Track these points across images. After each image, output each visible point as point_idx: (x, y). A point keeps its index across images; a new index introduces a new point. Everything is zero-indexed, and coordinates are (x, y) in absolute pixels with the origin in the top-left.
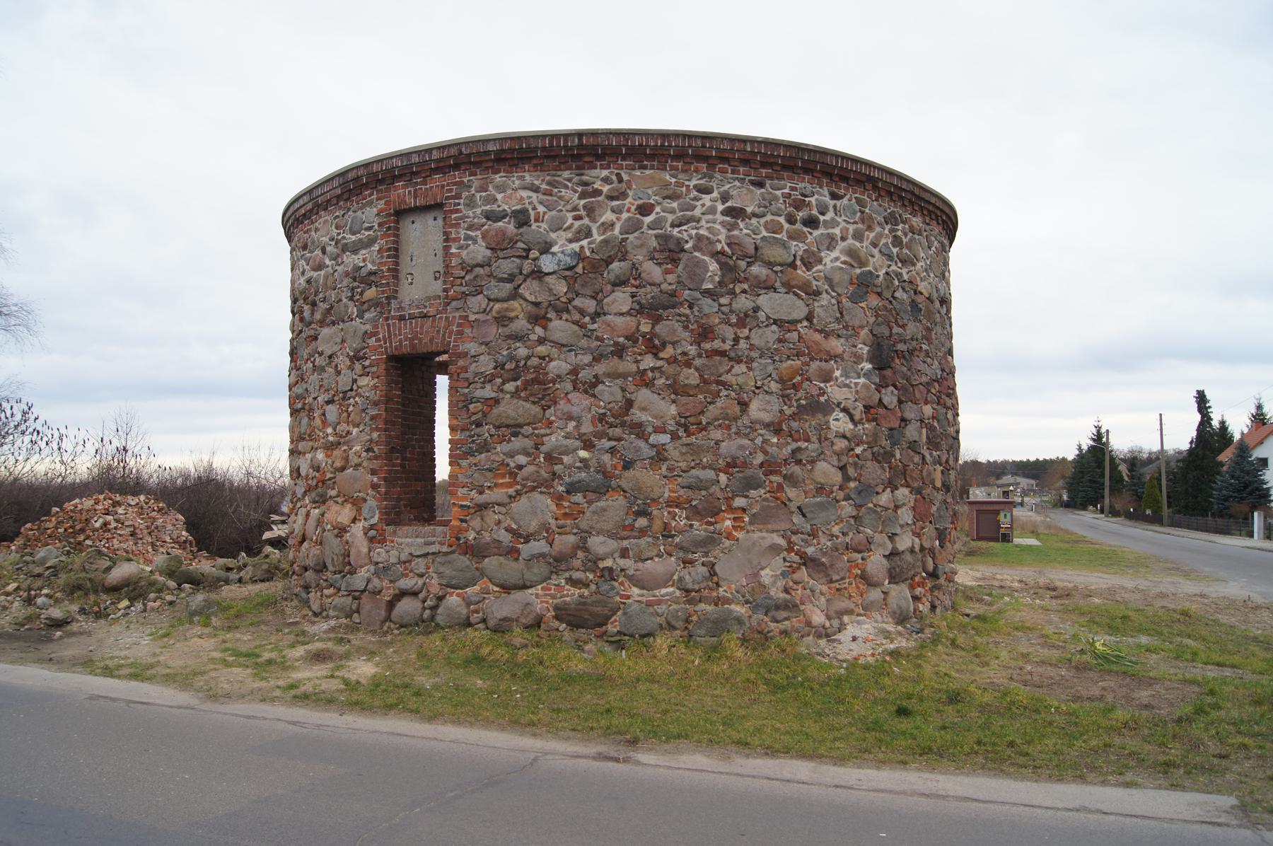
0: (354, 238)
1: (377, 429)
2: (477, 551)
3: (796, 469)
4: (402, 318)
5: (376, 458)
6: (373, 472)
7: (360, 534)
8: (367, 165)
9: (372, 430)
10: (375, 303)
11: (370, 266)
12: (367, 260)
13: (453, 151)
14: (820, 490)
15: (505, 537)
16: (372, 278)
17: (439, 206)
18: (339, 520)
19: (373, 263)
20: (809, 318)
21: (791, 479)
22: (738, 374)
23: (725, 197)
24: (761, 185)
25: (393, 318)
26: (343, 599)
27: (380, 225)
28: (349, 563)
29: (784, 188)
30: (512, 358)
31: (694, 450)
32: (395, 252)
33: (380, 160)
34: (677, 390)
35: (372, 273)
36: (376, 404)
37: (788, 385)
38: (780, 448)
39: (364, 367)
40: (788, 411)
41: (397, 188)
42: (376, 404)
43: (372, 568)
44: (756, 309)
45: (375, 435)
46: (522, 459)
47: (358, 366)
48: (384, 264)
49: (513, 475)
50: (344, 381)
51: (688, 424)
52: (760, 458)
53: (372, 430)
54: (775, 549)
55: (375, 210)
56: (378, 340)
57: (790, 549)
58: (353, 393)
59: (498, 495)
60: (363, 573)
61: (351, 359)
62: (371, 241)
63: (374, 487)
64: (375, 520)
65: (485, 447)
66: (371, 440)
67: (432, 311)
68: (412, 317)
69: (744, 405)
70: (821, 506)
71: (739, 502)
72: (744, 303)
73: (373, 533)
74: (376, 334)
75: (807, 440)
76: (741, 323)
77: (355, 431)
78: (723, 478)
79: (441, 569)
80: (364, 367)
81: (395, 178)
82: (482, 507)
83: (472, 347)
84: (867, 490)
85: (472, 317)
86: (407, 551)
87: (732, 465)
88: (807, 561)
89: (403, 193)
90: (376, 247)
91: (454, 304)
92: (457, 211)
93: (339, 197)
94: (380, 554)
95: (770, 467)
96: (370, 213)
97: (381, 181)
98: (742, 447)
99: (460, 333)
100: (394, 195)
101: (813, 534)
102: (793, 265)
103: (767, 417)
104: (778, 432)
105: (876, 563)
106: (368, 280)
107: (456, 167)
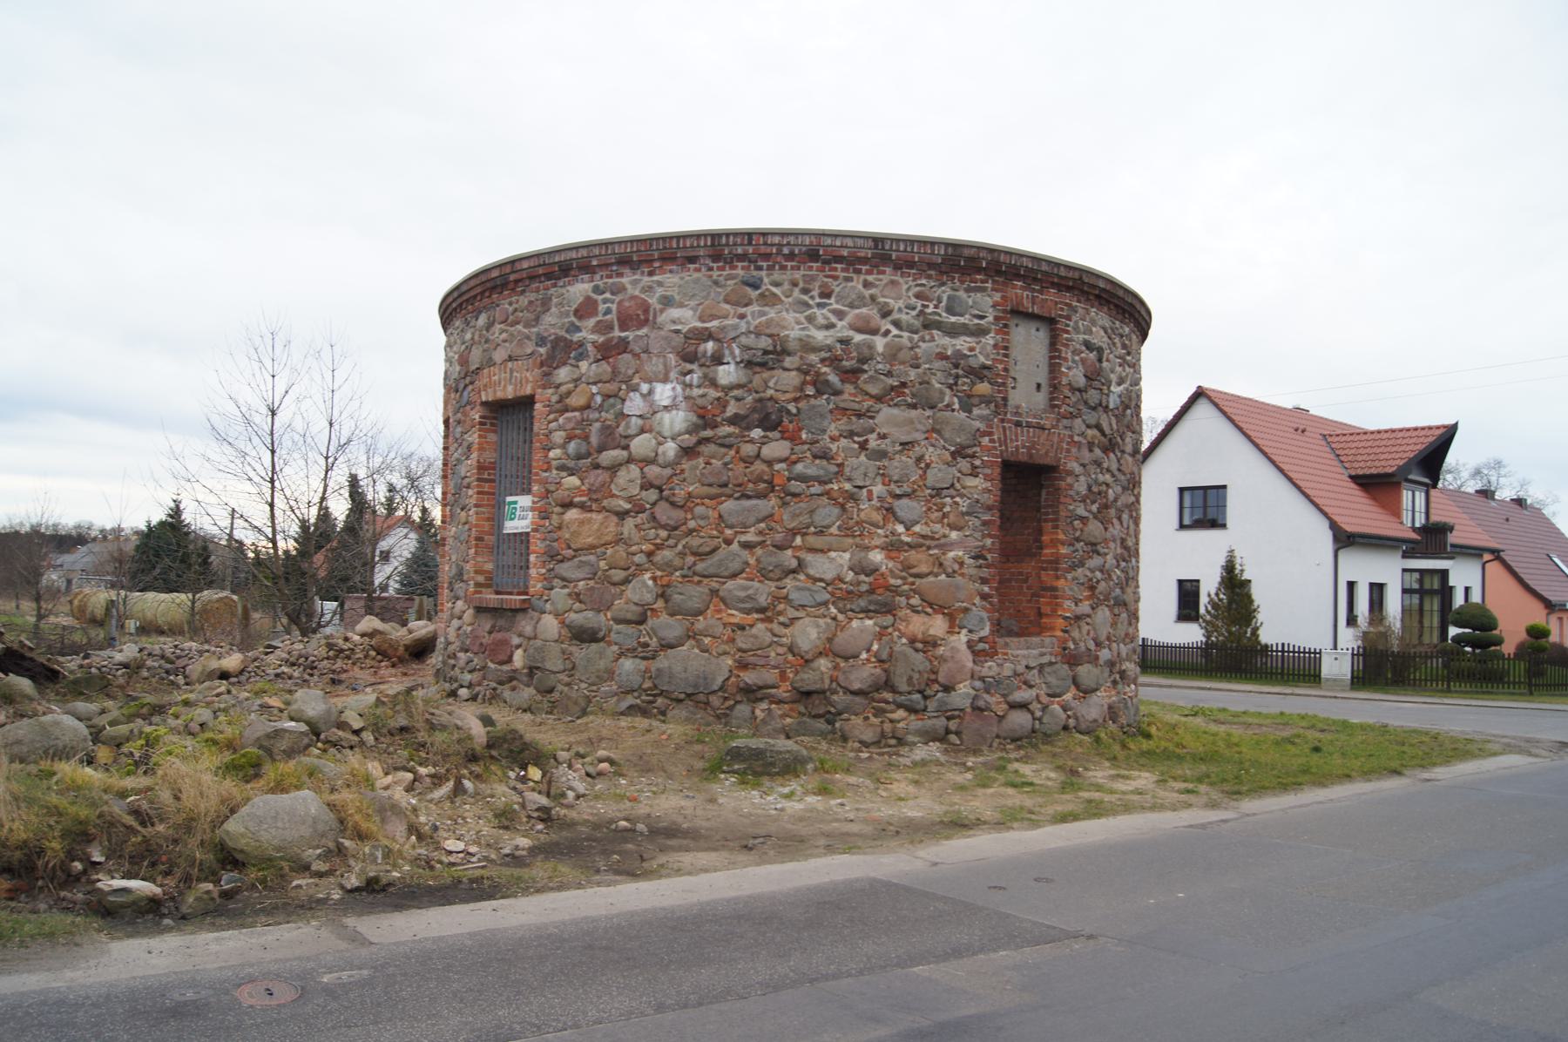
0: (953, 319)
1: (990, 536)
2: (1073, 660)
4: (1018, 424)
5: (988, 566)
6: (984, 581)
7: (964, 647)
8: (992, 250)
9: (984, 536)
10: (986, 400)
11: (982, 359)
12: (981, 351)
13: (1076, 275)
15: (1092, 645)
16: (986, 372)
17: (1050, 322)
18: (932, 632)
19: (987, 356)
25: (1009, 421)
26: (934, 721)
27: (997, 318)
28: (936, 681)
30: (1096, 481)
32: (1004, 348)
33: (1009, 253)
35: (985, 367)
36: (989, 508)
39: (974, 467)
41: (1015, 287)
42: (989, 508)
43: (978, 684)
45: (989, 542)
46: (1098, 574)
47: (964, 464)
48: (1001, 362)
49: (1092, 588)
50: (939, 474)
53: (984, 536)
55: (989, 301)
56: (992, 441)
58: (952, 491)
59: (1085, 608)
60: (964, 689)
61: (953, 454)
62: (980, 332)
63: (984, 597)
64: (986, 632)
65: (1082, 564)
66: (983, 547)
67: (1047, 423)
68: (1029, 425)
73: (981, 646)
74: (990, 434)
77: (954, 535)
79: (1049, 679)
80: (974, 467)
81: (1018, 276)
82: (1078, 618)
83: (1078, 469)
85: (1076, 438)
86: (1024, 663)
89: (1019, 292)
90: (989, 340)
91: (1065, 422)
92: (1067, 332)
93: (931, 265)
94: (990, 668)
96: (984, 302)
97: (999, 273)
99: (1068, 451)
100: (1011, 293)
106: (979, 373)
107: (1069, 289)
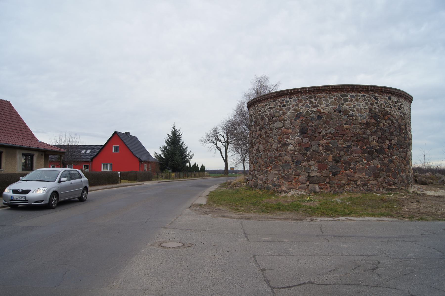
3: (280, 158)
14: (286, 162)
20: (284, 126)
21: (280, 160)
22: (270, 140)
23: (269, 105)
24: (275, 101)
29: (280, 100)
31: (265, 155)
34: (263, 144)
37: (279, 141)
38: (277, 154)
40: (279, 146)
44: (274, 126)
51: (265, 150)
52: (274, 156)
54: (276, 174)
57: (279, 174)
69: (272, 146)
70: (286, 165)
71: (271, 165)
72: (272, 125)
75: (283, 152)
76: (271, 130)
78: (268, 160)
84: (298, 163)
87: (270, 158)
88: (283, 177)
95: (275, 158)
98: (271, 154)
101: (284, 171)
102: (281, 116)
103: (275, 148)
104: (277, 150)
105: (302, 178)
